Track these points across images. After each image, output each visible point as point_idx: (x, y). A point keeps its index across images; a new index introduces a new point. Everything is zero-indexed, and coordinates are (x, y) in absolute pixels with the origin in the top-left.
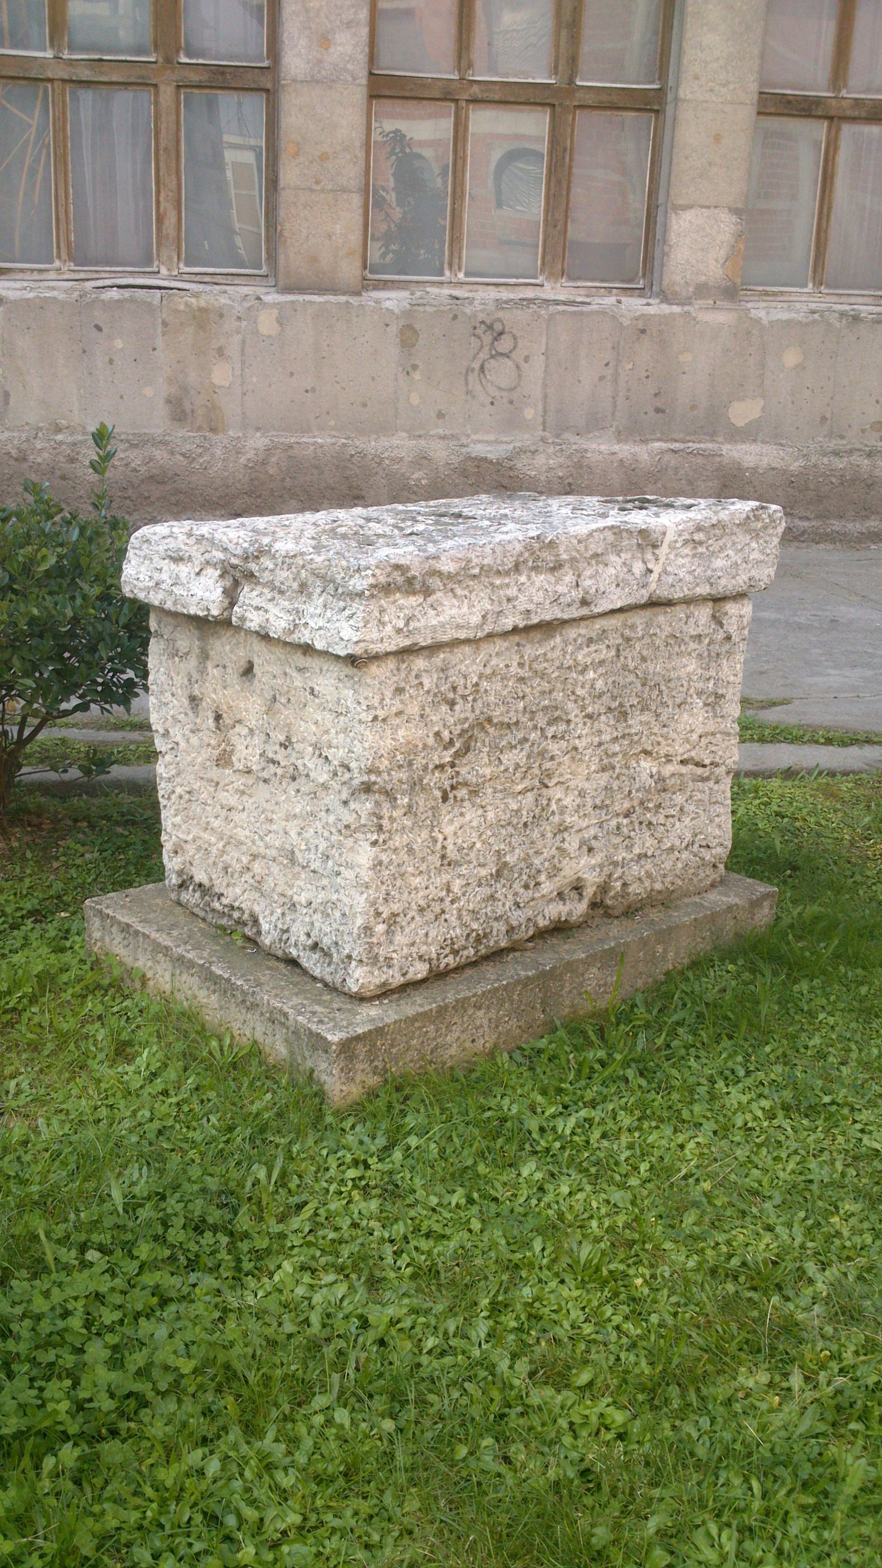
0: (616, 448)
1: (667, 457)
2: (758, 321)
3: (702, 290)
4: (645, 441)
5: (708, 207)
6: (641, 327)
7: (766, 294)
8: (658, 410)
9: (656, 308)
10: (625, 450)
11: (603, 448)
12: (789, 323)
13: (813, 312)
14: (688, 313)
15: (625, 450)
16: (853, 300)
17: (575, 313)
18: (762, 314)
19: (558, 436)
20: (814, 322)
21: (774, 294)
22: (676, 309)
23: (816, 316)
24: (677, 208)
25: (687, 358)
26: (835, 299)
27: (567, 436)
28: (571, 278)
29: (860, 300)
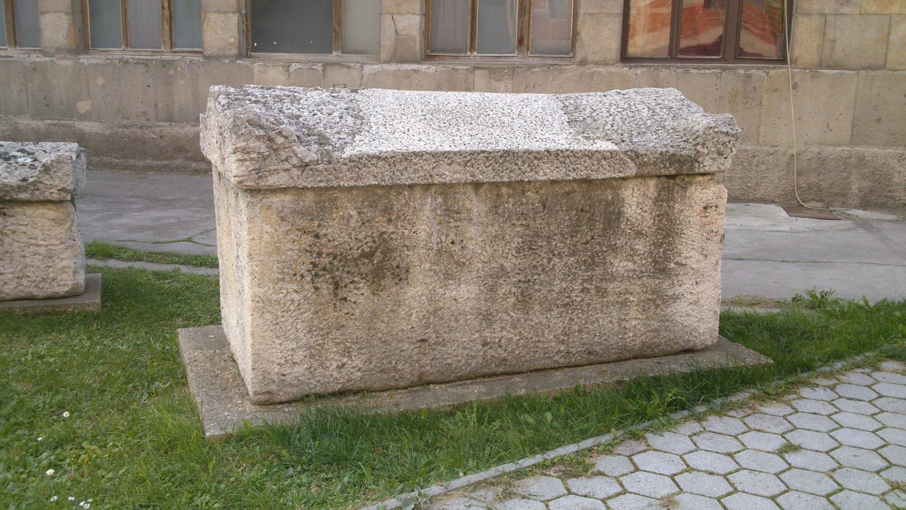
0: (30, 122)
1: (51, 127)
2: (82, 64)
3: (58, 50)
4: (43, 120)
5: (55, 12)
6: (33, 67)
7: (102, 51)
8: (46, 105)
9: (36, 58)
10: (34, 123)
11: (25, 122)
12: (96, 65)
13: (107, 59)
14: (53, 61)
15: (34, 123)
16: (142, 53)
17: (4, 61)
18: (85, 61)
19: (6, 116)
20: (108, 64)
21: (106, 52)
22: (48, 59)
23: (109, 61)
24: (42, 13)
25: (55, 81)
26: (133, 53)
27: (10, 116)
28: (20, 46)
29: (145, 53)
